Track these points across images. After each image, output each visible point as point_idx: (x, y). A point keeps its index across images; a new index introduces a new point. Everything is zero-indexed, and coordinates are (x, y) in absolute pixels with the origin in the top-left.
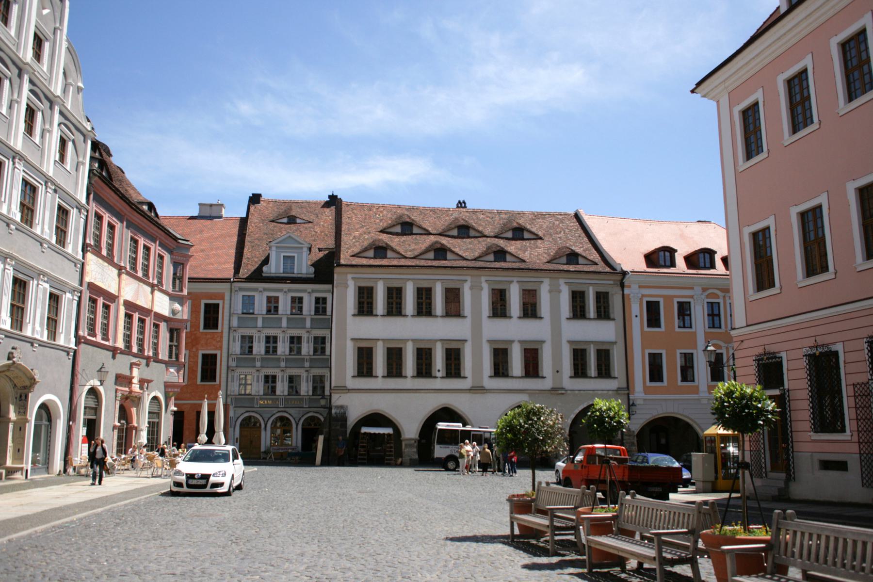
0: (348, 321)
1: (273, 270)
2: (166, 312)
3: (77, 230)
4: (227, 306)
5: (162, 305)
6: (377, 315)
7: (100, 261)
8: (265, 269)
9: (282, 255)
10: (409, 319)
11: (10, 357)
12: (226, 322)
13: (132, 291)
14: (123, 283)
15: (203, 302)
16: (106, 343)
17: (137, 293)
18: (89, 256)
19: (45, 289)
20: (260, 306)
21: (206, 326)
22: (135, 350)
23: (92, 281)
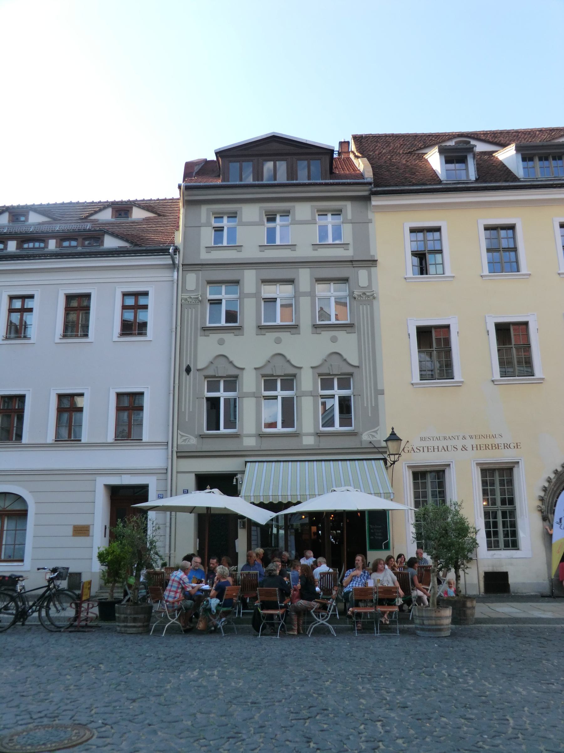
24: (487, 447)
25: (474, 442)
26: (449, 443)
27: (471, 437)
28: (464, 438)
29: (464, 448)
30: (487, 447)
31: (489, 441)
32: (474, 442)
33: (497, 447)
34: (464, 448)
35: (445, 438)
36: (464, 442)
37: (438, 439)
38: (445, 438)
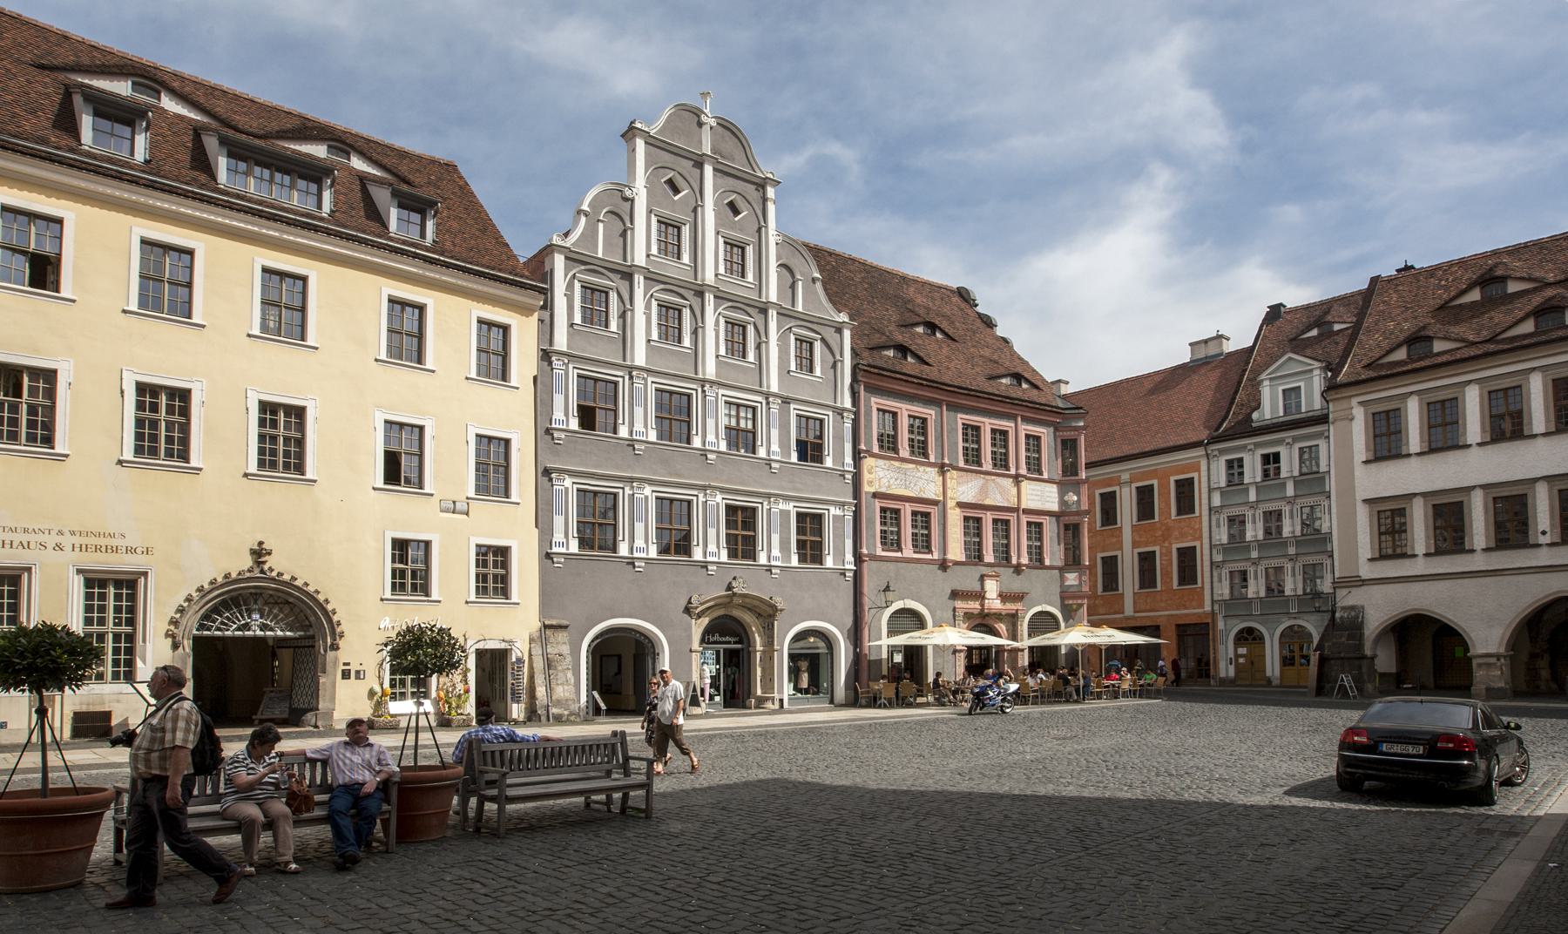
0: (1357, 473)
1: (1268, 416)
2: (1055, 507)
3: (839, 438)
4: (1204, 479)
5: (1042, 496)
6: (1409, 455)
7: (897, 464)
8: (1255, 416)
9: (1281, 388)
10: (1475, 452)
11: (729, 588)
12: (1205, 501)
13: (965, 488)
14: (949, 483)
15: (1173, 479)
16: (929, 556)
17: (983, 490)
18: (868, 462)
19: (785, 514)
20: (1253, 470)
21: (1179, 513)
22: (989, 557)
23: (883, 490)
24: (97, 549)
25: (77, 540)
26: (32, 538)
27: (73, 533)
28: (60, 533)
29: (59, 547)
30: (97, 549)
31: (102, 542)
32: (77, 540)
33: (116, 550)
34: (59, 547)
35: (25, 531)
36: (59, 539)
37: (14, 530)
38: (25, 531)
